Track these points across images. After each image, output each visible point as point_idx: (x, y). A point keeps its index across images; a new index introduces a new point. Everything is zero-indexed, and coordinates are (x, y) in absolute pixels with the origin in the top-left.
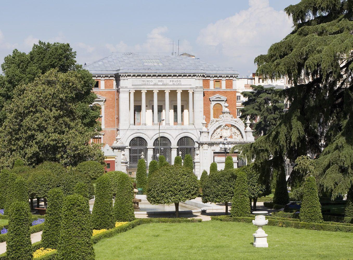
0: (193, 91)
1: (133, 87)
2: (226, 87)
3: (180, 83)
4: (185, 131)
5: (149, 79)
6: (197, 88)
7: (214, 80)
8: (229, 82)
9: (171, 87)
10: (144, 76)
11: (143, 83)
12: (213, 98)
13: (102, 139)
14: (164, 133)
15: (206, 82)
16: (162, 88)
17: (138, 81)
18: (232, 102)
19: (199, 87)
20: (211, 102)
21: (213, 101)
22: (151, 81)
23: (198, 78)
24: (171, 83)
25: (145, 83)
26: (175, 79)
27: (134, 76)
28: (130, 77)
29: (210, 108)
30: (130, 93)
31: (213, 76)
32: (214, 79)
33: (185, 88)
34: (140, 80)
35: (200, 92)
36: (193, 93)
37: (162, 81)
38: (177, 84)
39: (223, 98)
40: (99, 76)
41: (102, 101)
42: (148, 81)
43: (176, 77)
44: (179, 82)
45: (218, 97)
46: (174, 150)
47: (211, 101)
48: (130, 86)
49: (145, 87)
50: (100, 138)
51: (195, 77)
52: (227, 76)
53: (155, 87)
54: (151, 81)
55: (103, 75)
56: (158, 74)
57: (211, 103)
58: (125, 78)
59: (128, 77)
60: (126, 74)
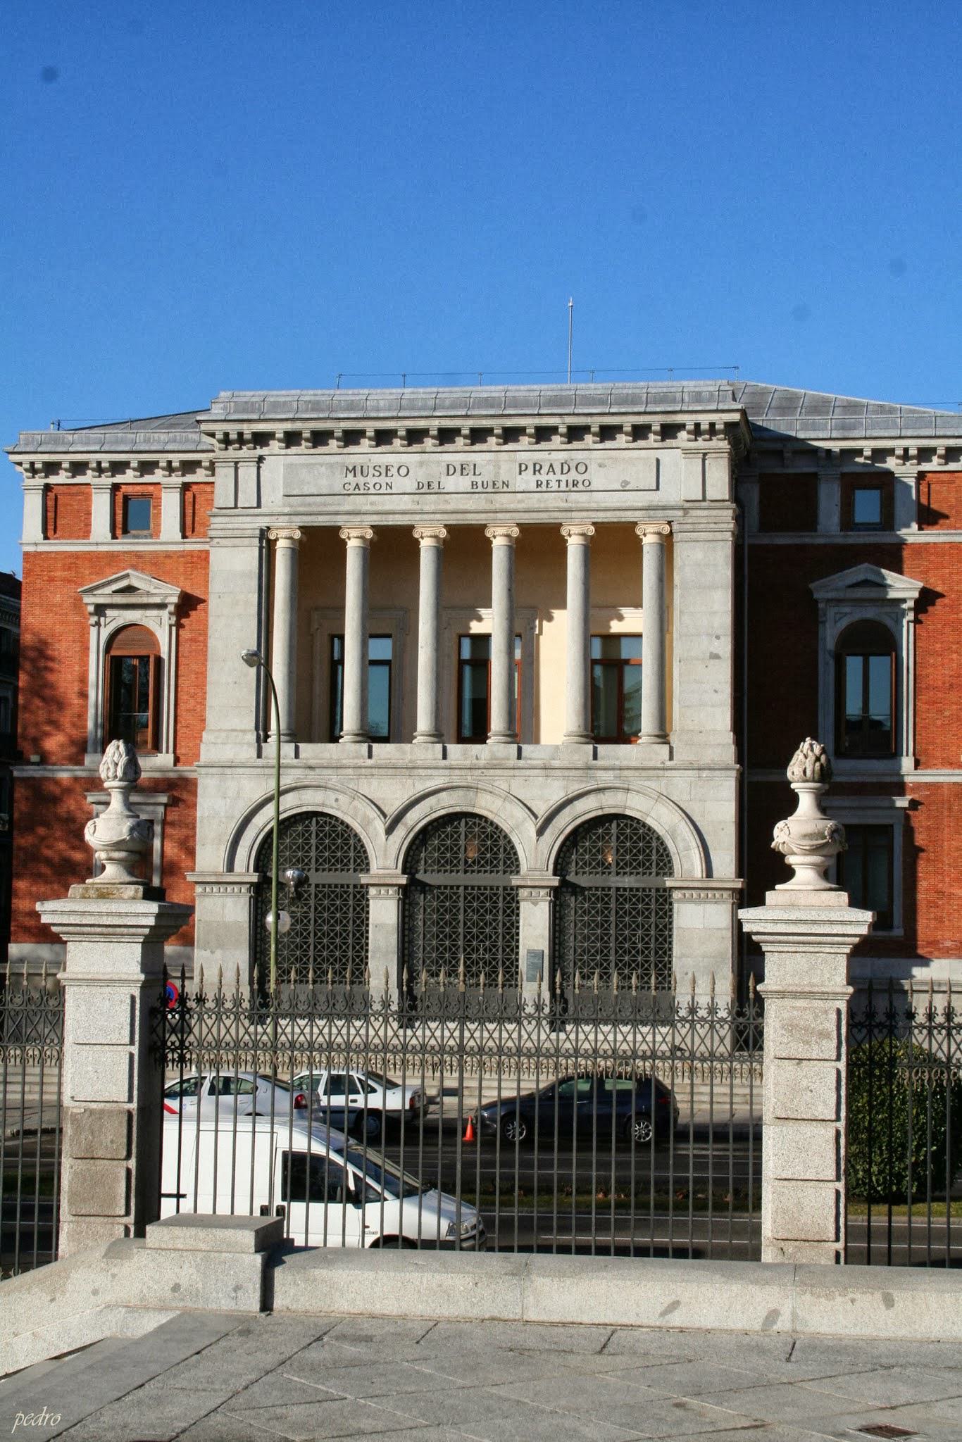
0: (666, 530)
1: (287, 510)
9: (521, 506)
16: (470, 509)
17: (323, 469)
22: (403, 471)
23: (701, 443)
29: (816, 652)
30: (267, 547)
35: (710, 536)
41: (162, 606)
44: (573, 475)
47: (821, 606)
54: (403, 471)
55: (170, 456)
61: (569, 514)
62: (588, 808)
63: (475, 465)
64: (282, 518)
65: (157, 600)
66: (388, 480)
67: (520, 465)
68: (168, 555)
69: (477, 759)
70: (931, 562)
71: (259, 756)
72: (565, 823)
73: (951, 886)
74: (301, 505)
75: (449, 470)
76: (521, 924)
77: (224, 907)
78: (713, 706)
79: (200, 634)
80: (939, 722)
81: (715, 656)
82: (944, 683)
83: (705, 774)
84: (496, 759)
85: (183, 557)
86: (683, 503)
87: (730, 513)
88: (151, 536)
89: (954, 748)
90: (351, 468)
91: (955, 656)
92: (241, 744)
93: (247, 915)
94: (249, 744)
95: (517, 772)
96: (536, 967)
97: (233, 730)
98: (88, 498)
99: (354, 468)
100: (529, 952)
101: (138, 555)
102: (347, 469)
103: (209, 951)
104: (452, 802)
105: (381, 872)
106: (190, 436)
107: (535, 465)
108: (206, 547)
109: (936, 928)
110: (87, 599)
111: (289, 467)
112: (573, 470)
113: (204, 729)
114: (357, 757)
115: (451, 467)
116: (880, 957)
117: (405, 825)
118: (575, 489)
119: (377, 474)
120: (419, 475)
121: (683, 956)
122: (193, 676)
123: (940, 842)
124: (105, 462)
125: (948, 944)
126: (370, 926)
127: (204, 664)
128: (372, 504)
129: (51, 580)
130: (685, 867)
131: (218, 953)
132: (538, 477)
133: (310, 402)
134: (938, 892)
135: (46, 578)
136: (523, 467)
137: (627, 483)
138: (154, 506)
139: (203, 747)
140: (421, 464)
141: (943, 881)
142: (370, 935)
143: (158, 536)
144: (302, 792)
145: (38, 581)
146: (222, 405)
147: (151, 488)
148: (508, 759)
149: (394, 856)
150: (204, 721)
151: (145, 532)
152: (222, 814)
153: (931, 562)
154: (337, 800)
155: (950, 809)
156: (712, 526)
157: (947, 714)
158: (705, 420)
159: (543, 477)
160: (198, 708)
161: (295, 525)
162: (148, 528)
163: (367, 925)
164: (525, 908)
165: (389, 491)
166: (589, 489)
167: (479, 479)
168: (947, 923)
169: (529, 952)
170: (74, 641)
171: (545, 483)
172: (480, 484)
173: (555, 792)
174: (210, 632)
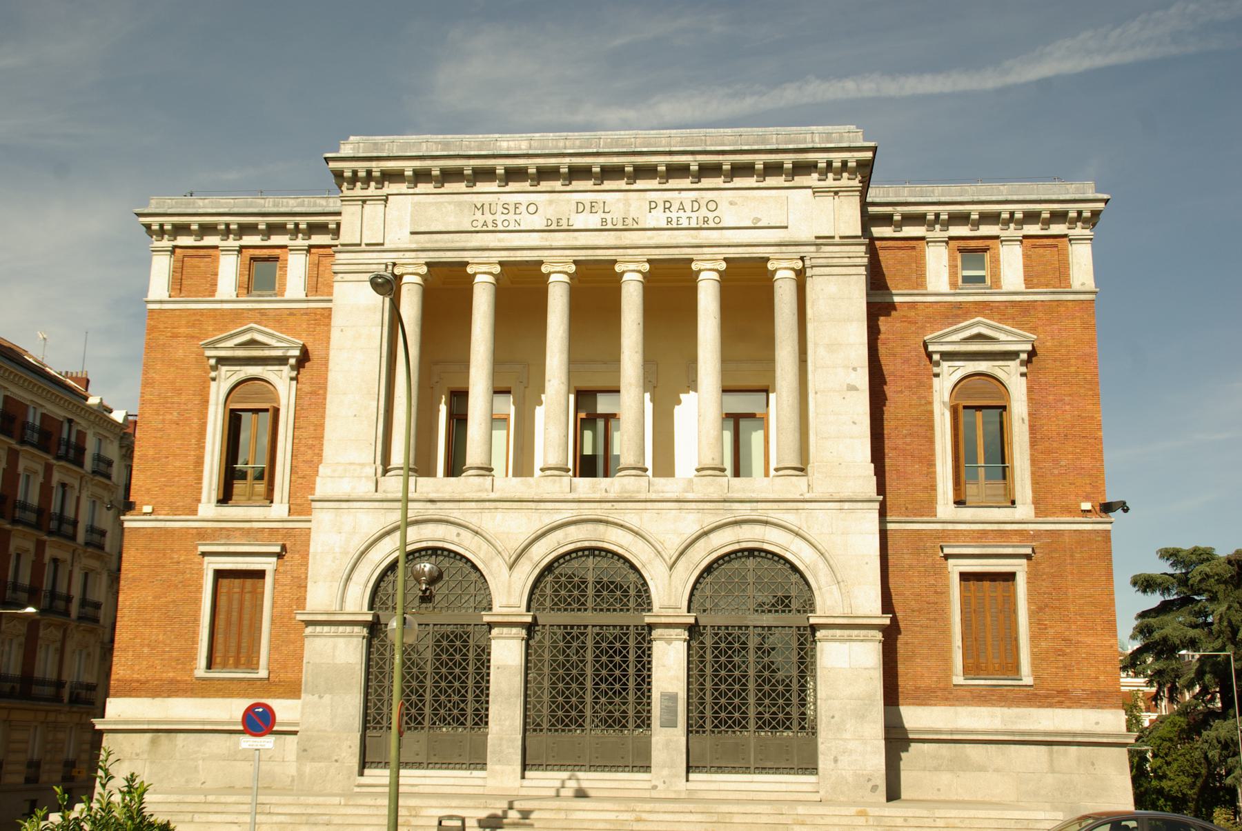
0: (799, 265)
1: (414, 246)
2: (1028, 281)
3: (711, 215)
4: (744, 511)
5: (518, 195)
6: (822, 241)
7: (951, 243)
8: (1048, 251)
10: (485, 174)
11: (481, 219)
12: (953, 339)
13: (269, 579)
14: (600, 521)
15: (900, 253)
16: (599, 245)
18: (1073, 369)
19: (837, 240)
20: (937, 364)
21: (948, 356)
22: (532, 209)
23: (830, 181)
24: (658, 218)
25: (489, 218)
26: (682, 193)
27: (421, 176)
28: (403, 187)
29: (931, 403)
31: (944, 217)
32: (951, 238)
33: (745, 243)
34: (460, 204)
36: (801, 277)
38: (693, 225)
39: (1010, 338)
40: (273, 229)
41: (282, 361)
42: (512, 208)
43: (686, 183)
45: (980, 337)
46: (669, 641)
47: (936, 357)
48: (399, 236)
49: (492, 245)
50: (260, 574)
51: (813, 179)
52: (1031, 217)
53: (555, 244)
54: (532, 209)
55: (298, 219)
56: (567, 160)
57: (936, 370)
58: (372, 190)
59: (390, 188)
60: (374, 164)
61: (699, 250)
62: (724, 541)
63: (604, 203)
64: (408, 255)
65: (279, 353)
66: (517, 217)
67: (650, 202)
68: (292, 313)
69: (606, 491)
70: (1039, 319)
72: (701, 556)
74: (427, 243)
75: (579, 208)
76: (654, 663)
77: (334, 647)
78: (851, 438)
79: (321, 388)
80: (1056, 472)
81: (852, 388)
82: (1058, 434)
83: (846, 505)
84: (626, 492)
85: (306, 314)
86: (813, 239)
87: (863, 248)
88: (276, 295)
89: (1072, 497)
91: (1068, 407)
92: (360, 477)
93: (359, 656)
94: (367, 477)
95: (649, 505)
96: (670, 711)
97: (351, 464)
98: (216, 260)
99: (483, 206)
100: (662, 695)
101: (262, 312)
102: (476, 206)
103: (317, 696)
104: (581, 537)
105: (505, 610)
106: (318, 201)
107: (665, 202)
108: (333, 204)
109: (1065, 678)
110: (208, 353)
111: (415, 205)
112: (704, 209)
113: (320, 462)
114: (480, 491)
116: (1009, 706)
117: (531, 560)
118: (706, 226)
119: (506, 211)
120: (551, 212)
121: (829, 698)
122: (312, 428)
124: (234, 224)
125: (1079, 693)
126: (492, 668)
127: (323, 417)
128: (499, 241)
129: (175, 336)
130: (828, 603)
131: (327, 698)
132: (668, 214)
133: (440, 143)
134: (1067, 640)
135: (169, 334)
136: (653, 205)
137: (759, 220)
138: (280, 267)
139: (318, 480)
140: (551, 202)
141: (1069, 629)
142: (492, 678)
143: (282, 294)
144: (422, 526)
145: (161, 338)
146: (351, 146)
147: (277, 252)
148: (639, 492)
149: (518, 594)
150: (318, 471)
151: (271, 292)
152: (337, 550)
153: (1039, 319)
154: (458, 535)
155: (1072, 556)
156: (847, 260)
157: (1063, 463)
158: (837, 158)
159: (674, 215)
160: (316, 459)
161: (423, 261)
162: (274, 289)
163: (489, 668)
164: (658, 648)
165: (518, 228)
166: (719, 226)
167: (608, 217)
168: (1076, 672)
169: (662, 695)
170: (194, 395)
171: (675, 220)
172: (609, 221)
173: (691, 523)
174: (331, 365)
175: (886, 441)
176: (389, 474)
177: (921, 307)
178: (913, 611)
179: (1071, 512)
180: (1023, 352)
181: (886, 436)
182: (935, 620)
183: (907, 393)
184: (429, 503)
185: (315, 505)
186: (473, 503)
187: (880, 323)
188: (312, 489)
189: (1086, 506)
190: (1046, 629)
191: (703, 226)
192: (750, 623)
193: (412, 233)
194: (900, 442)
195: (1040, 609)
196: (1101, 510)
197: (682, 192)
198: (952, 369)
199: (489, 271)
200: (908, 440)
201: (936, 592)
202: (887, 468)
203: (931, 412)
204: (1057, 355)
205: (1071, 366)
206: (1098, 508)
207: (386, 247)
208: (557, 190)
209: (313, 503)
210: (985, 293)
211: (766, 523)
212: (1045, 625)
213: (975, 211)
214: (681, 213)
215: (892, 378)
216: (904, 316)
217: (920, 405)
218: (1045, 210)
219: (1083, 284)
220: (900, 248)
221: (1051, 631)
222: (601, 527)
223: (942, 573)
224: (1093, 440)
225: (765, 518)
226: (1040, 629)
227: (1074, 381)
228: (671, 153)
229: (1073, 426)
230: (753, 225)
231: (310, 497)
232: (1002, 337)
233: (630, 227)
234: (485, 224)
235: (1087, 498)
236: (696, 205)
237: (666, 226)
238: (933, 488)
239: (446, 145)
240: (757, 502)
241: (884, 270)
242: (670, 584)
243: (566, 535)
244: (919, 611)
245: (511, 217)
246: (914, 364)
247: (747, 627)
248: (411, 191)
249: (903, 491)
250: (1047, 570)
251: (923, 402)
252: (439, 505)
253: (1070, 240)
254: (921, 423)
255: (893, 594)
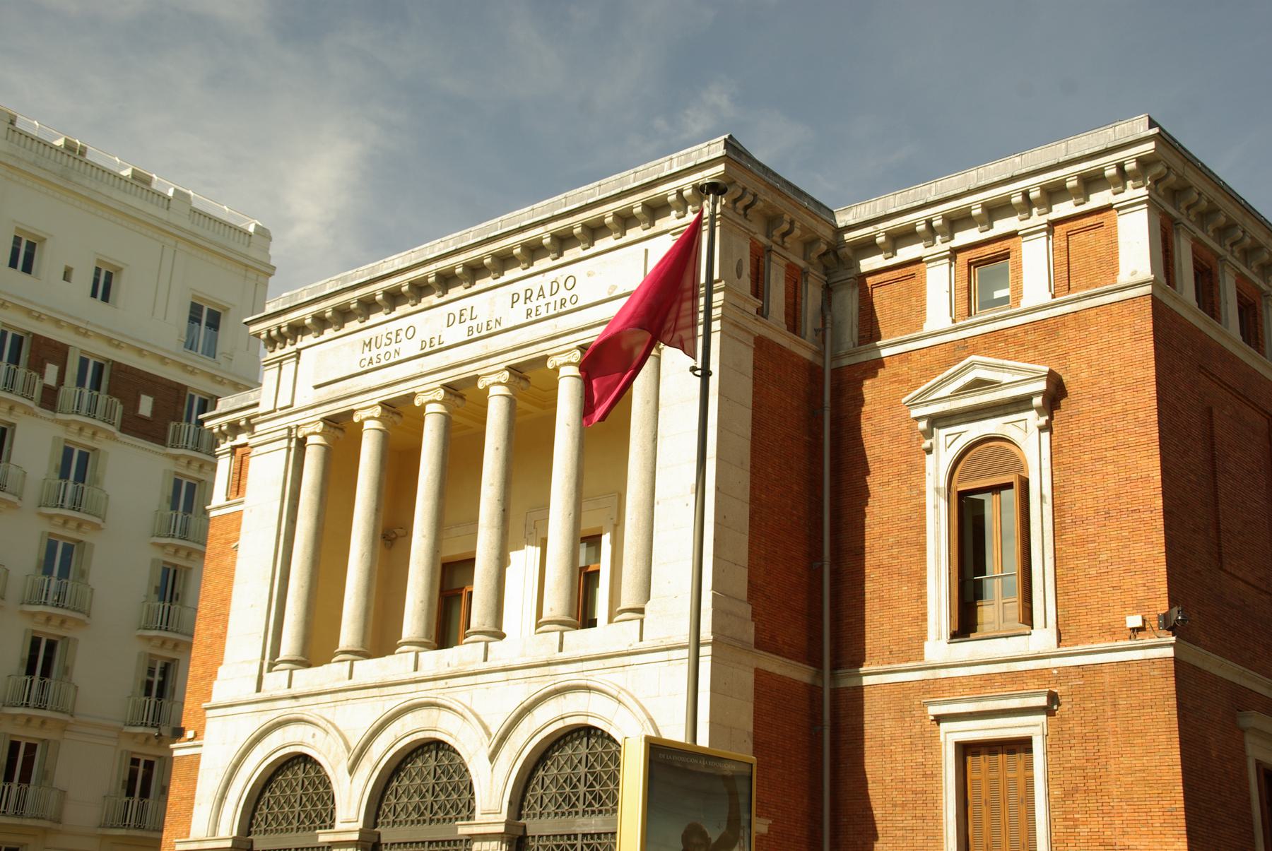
4: (567, 675)
18: (1118, 408)
27: (321, 322)
28: (309, 339)
37: (467, 314)
38: (552, 312)
42: (393, 337)
48: (306, 396)
52: (1054, 193)
54: (410, 335)
71: (259, 690)
73: (1124, 834)
80: (1093, 572)
82: (1096, 512)
89: (1117, 609)
90: (367, 342)
91: (1110, 468)
115: (452, 317)
118: (564, 309)
119: (388, 342)
123: (1103, 761)
132: (529, 305)
136: (516, 296)
137: (614, 287)
148: (474, 662)
155: (1114, 705)
157: (1103, 557)
166: (576, 306)
175: (868, 557)
176: (274, 669)
177: (915, 356)
178: (895, 805)
179: (1114, 633)
180: (1037, 394)
181: (867, 550)
182: (923, 818)
183: (895, 484)
184: (293, 700)
185: (209, 713)
186: (329, 696)
187: (865, 391)
188: (208, 695)
189: (1134, 621)
190: (1076, 827)
191: (561, 311)
192: (579, 830)
193: (316, 387)
194: (884, 555)
195: (1068, 794)
196: (1159, 625)
197: (546, 274)
198: (950, 439)
199: (371, 415)
200: (895, 551)
201: (925, 776)
202: (868, 596)
203: (923, 506)
204: (1096, 390)
205: (1116, 402)
206: (1155, 624)
207: (296, 407)
208: (434, 304)
209: (208, 712)
210: (995, 318)
211: (588, 689)
212: (1075, 820)
213: (975, 203)
214: (542, 301)
215: (878, 465)
216: (895, 375)
217: (912, 498)
218: (1070, 175)
219: (1133, 273)
220: (896, 280)
221: (1083, 830)
222: (434, 712)
223: (930, 745)
224: (1147, 515)
225: (583, 683)
226: (1067, 827)
227: (1119, 425)
228: (522, 229)
229: (1118, 496)
230: (608, 296)
231: (205, 705)
232: (1005, 377)
233: (494, 330)
234: (371, 362)
235: (1137, 609)
236: (555, 285)
237: (526, 321)
238: (924, 617)
239: (344, 280)
240: (582, 660)
241: (878, 314)
242: (492, 781)
243: (403, 725)
244: (903, 805)
245: (394, 346)
246: (905, 440)
247: (576, 836)
248: (318, 340)
249: (887, 627)
250: (1077, 730)
251: (915, 492)
252: (302, 701)
253: (1118, 209)
254: (911, 524)
255: (870, 782)
